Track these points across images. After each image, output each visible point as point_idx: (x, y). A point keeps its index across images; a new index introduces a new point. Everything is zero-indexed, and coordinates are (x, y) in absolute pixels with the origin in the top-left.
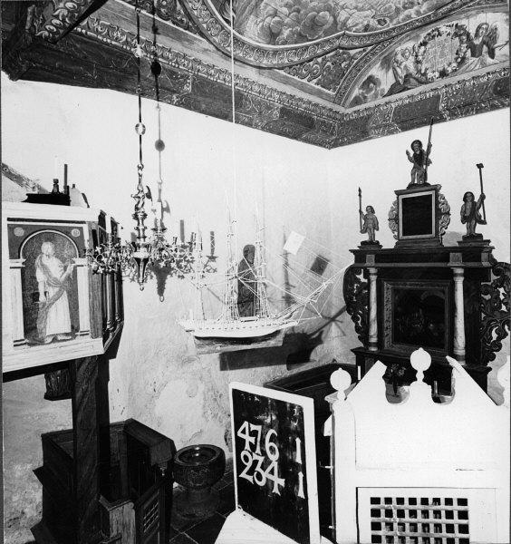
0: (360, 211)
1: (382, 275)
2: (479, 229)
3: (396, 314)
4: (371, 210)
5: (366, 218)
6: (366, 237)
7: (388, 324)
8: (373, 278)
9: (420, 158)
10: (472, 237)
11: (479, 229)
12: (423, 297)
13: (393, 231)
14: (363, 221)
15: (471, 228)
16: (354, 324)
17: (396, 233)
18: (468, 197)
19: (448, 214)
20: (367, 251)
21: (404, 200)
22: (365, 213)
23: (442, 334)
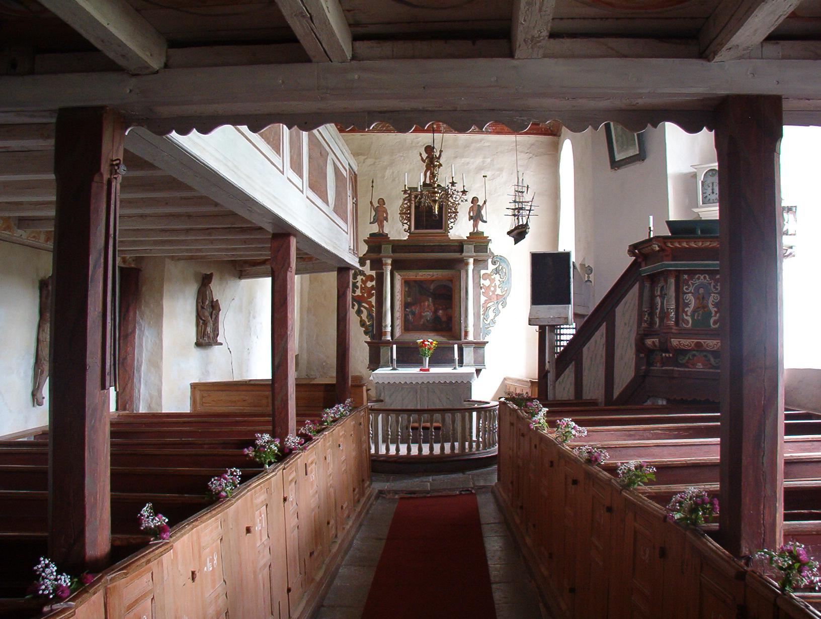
0: (371, 203)
1: (397, 266)
2: (481, 227)
3: (406, 305)
4: (382, 202)
5: (376, 210)
6: (375, 229)
7: (398, 314)
8: (389, 268)
9: (431, 160)
11: (481, 227)
12: (432, 287)
13: (403, 223)
14: (373, 213)
15: (475, 225)
17: (406, 227)
19: (456, 212)
20: (377, 243)
23: (450, 319)
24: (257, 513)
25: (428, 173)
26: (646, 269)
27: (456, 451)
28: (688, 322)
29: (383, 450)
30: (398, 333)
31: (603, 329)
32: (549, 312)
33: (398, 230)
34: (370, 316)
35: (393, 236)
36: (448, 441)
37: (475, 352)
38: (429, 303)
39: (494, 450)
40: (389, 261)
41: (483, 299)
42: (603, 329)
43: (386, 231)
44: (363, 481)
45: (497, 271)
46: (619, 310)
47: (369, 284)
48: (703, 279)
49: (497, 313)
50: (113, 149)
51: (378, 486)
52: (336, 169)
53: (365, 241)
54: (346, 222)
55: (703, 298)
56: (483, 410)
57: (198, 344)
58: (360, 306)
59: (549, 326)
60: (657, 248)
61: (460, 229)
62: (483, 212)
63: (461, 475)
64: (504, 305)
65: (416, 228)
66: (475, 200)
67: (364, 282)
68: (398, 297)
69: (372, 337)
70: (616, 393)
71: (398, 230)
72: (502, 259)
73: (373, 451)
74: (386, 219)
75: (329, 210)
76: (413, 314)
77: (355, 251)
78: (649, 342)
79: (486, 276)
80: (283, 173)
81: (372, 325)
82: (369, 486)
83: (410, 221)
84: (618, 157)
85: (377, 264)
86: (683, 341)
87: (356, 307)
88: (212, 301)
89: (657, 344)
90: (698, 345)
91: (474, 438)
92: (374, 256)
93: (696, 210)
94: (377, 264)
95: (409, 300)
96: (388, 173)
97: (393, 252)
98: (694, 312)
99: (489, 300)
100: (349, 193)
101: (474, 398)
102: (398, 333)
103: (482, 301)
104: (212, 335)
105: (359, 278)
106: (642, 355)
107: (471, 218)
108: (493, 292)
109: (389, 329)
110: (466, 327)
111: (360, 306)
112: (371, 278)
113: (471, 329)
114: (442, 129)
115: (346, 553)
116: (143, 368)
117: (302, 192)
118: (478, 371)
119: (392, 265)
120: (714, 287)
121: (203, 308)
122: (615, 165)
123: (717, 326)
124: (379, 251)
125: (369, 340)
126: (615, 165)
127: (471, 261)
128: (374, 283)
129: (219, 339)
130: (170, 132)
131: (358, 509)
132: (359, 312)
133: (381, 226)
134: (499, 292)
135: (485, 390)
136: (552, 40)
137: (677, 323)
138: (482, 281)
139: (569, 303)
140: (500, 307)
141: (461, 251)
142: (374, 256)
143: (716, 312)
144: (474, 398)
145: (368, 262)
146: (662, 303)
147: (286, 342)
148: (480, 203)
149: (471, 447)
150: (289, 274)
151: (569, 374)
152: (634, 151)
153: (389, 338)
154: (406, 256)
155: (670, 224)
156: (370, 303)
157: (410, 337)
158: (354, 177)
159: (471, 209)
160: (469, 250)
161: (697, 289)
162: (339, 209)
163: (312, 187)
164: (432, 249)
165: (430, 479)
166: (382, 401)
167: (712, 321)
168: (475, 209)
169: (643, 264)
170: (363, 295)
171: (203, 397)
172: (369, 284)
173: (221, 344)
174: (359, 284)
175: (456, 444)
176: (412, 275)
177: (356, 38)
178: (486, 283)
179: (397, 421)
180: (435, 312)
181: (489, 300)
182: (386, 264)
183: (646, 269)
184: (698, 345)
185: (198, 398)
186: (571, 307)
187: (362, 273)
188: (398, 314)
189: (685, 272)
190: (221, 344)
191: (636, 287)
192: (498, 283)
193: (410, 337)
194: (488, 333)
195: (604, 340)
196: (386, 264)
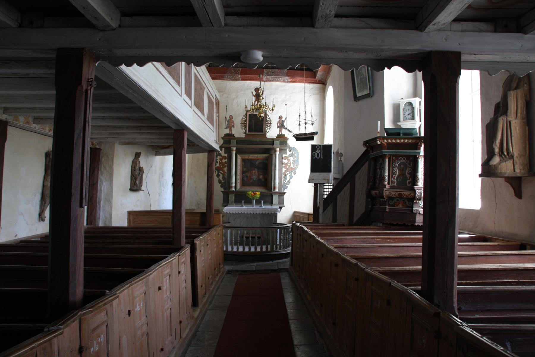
3: (243, 172)
4: (231, 117)
5: (228, 121)
6: (227, 131)
7: (239, 177)
8: (234, 152)
10: (281, 136)
11: (284, 132)
12: (257, 163)
14: (227, 123)
15: (280, 131)
16: (218, 179)
17: (244, 131)
18: (280, 117)
19: (270, 124)
21: (250, 115)
22: (228, 118)
24: (165, 279)
25: (256, 103)
26: (372, 154)
27: (269, 250)
28: (394, 183)
29: (230, 249)
30: (238, 187)
31: (348, 186)
32: (320, 176)
33: (239, 132)
34: (223, 177)
35: (237, 136)
36: (265, 245)
37: (279, 198)
38: (255, 172)
39: (289, 250)
40: (235, 149)
41: (284, 170)
42: (348, 186)
43: (233, 132)
44: (220, 264)
45: (291, 155)
46: (357, 176)
47: (224, 161)
48: (402, 160)
49: (291, 177)
50: (90, 71)
51: (227, 268)
52: (209, 97)
53: (222, 138)
54: (213, 125)
55: (403, 170)
56: (283, 228)
57: (131, 190)
58: (219, 172)
59: (320, 184)
60: (379, 143)
61: (272, 132)
62: (285, 124)
63: (271, 262)
64: (295, 173)
65: (249, 131)
66: (280, 117)
67: (221, 160)
68: (239, 168)
69: (225, 189)
70: (355, 219)
71: (239, 132)
72: (294, 149)
73: (225, 249)
74: (233, 126)
75: (205, 118)
76: (247, 177)
77: (217, 142)
78: (373, 193)
79: (286, 158)
80: (181, 96)
81: (225, 183)
82: (223, 267)
83: (246, 127)
84: (358, 95)
85: (228, 151)
86: (391, 192)
87: (217, 173)
88: (140, 167)
89: (378, 194)
90: (400, 195)
91: (278, 243)
92: (227, 146)
93: (399, 123)
94: (228, 151)
95: (245, 169)
96: (235, 102)
97: (237, 143)
98: (398, 177)
99: (287, 170)
100: (215, 110)
101: (278, 222)
102: (238, 187)
103: (283, 171)
104: (138, 185)
105: (219, 157)
106: (369, 200)
107: (278, 127)
108: (289, 166)
109: (234, 185)
110: (275, 184)
111: (219, 172)
112: (225, 158)
113: (277, 185)
114: (264, 79)
115: (211, 303)
116: (102, 202)
117: (191, 107)
118: (281, 208)
119: (236, 150)
120: (409, 164)
121: (135, 170)
122: (356, 99)
123: (410, 185)
124: (230, 143)
125: (222, 190)
126: (356, 99)
127: (278, 149)
128: (226, 160)
129: (143, 188)
130: (121, 65)
131: (217, 279)
132: (218, 176)
133: (231, 130)
134: (292, 166)
135: (283, 217)
136: (336, 19)
137: (389, 183)
138: (284, 161)
139: (330, 171)
140: (293, 174)
141: (273, 144)
142: (227, 146)
143: (410, 178)
144: (278, 222)
145: (223, 149)
146: (381, 172)
147: (181, 188)
148: (283, 119)
149: (276, 248)
150: (183, 151)
151: (330, 209)
152: (366, 92)
153: (234, 189)
154: (243, 146)
155: (386, 130)
156: (223, 171)
157: (244, 189)
158: (218, 103)
159: (279, 122)
160: (277, 143)
161: (400, 165)
162: (210, 119)
163: (196, 105)
164: (258, 143)
165: (255, 264)
166: (229, 223)
167: (407, 182)
168: (281, 122)
169: (371, 152)
170: (220, 167)
171: (134, 219)
172: (224, 161)
173: (143, 191)
174: (218, 161)
175: (269, 246)
176: (246, 156)
177: (227, 14)
178: (286, 161)
179: (237, 233)
180: (259, 175)
181: (287, 170)
182: (233, 150)
183: (372, 154)
184: (400, 195)
185: (132, 219)
186: (331, 174)
187: (220, 155)
188: (238, 177)
189: (393, 156)
190: (143, 191)
191: (367, 165)
192: (291, 161)
193: (244, 189)
194: (286, 188)
195: (349, 192)
196: (233, 150)
